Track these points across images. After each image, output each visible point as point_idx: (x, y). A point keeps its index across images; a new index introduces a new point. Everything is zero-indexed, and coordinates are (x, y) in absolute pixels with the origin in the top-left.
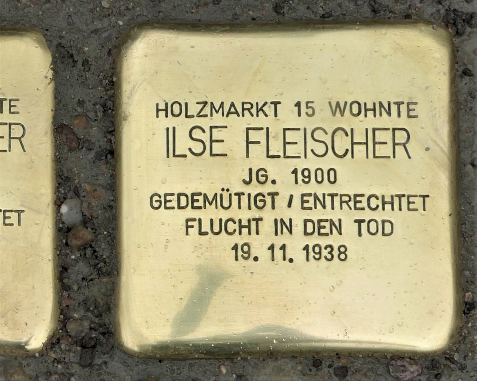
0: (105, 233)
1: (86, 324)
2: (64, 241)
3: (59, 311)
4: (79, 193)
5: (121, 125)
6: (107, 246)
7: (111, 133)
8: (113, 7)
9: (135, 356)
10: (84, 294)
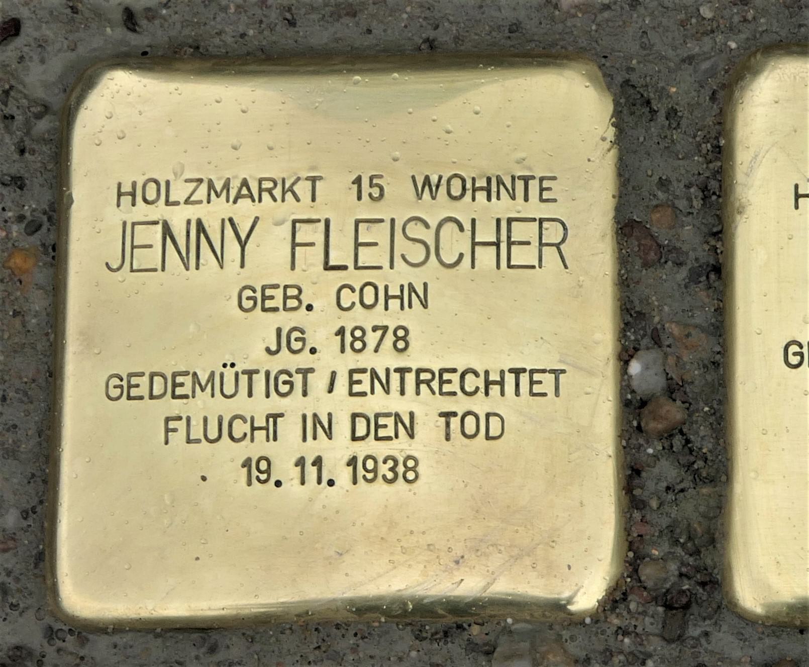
0: (706, 409)
1: (673, 567)
2: (635, 423)
3: (627, 544)
4: (660, 339)
5: (733, 221)
6: (709, 432)
7: (717, 237)
8: (720, 17)
9: (757, 623)
10: (669, 515)
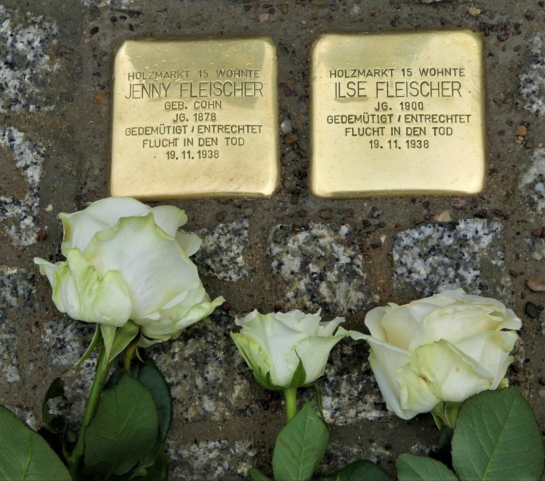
1: (294, 183)
